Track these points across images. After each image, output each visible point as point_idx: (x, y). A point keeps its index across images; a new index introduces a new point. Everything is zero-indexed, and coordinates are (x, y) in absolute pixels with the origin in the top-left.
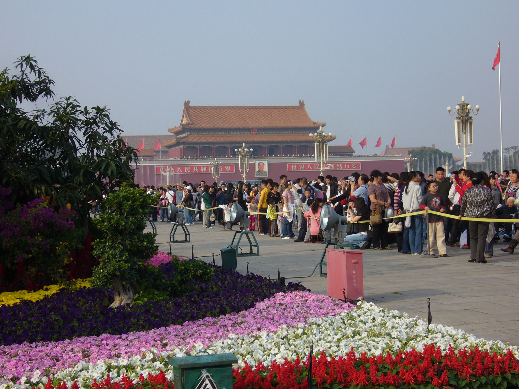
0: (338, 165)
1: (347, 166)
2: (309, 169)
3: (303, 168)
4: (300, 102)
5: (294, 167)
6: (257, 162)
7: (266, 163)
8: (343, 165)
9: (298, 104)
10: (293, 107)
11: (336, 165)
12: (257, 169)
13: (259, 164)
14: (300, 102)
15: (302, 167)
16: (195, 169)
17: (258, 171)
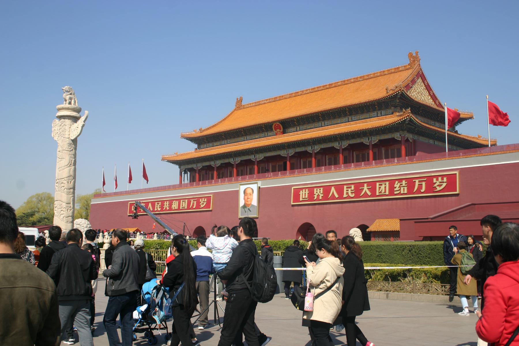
0: (397, 185)
1: (420, 186)
2: (333, 197)
3: (321, 195)
4: (410, 55)
5: (304, 194)
6: (242, 188)
7: (255, 187)
8: (410, 182)
9: (406, 62)
10: (397, 70)
11: (392, 183)
12: (242, 203)
13: (245, 192)
14: (410, 55)
15: (319, 193)
16: (166, 205)
17: (245, 206)
